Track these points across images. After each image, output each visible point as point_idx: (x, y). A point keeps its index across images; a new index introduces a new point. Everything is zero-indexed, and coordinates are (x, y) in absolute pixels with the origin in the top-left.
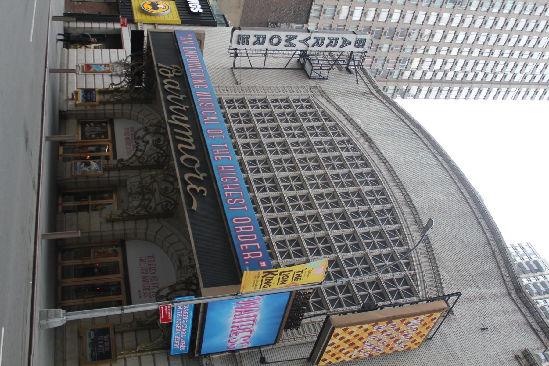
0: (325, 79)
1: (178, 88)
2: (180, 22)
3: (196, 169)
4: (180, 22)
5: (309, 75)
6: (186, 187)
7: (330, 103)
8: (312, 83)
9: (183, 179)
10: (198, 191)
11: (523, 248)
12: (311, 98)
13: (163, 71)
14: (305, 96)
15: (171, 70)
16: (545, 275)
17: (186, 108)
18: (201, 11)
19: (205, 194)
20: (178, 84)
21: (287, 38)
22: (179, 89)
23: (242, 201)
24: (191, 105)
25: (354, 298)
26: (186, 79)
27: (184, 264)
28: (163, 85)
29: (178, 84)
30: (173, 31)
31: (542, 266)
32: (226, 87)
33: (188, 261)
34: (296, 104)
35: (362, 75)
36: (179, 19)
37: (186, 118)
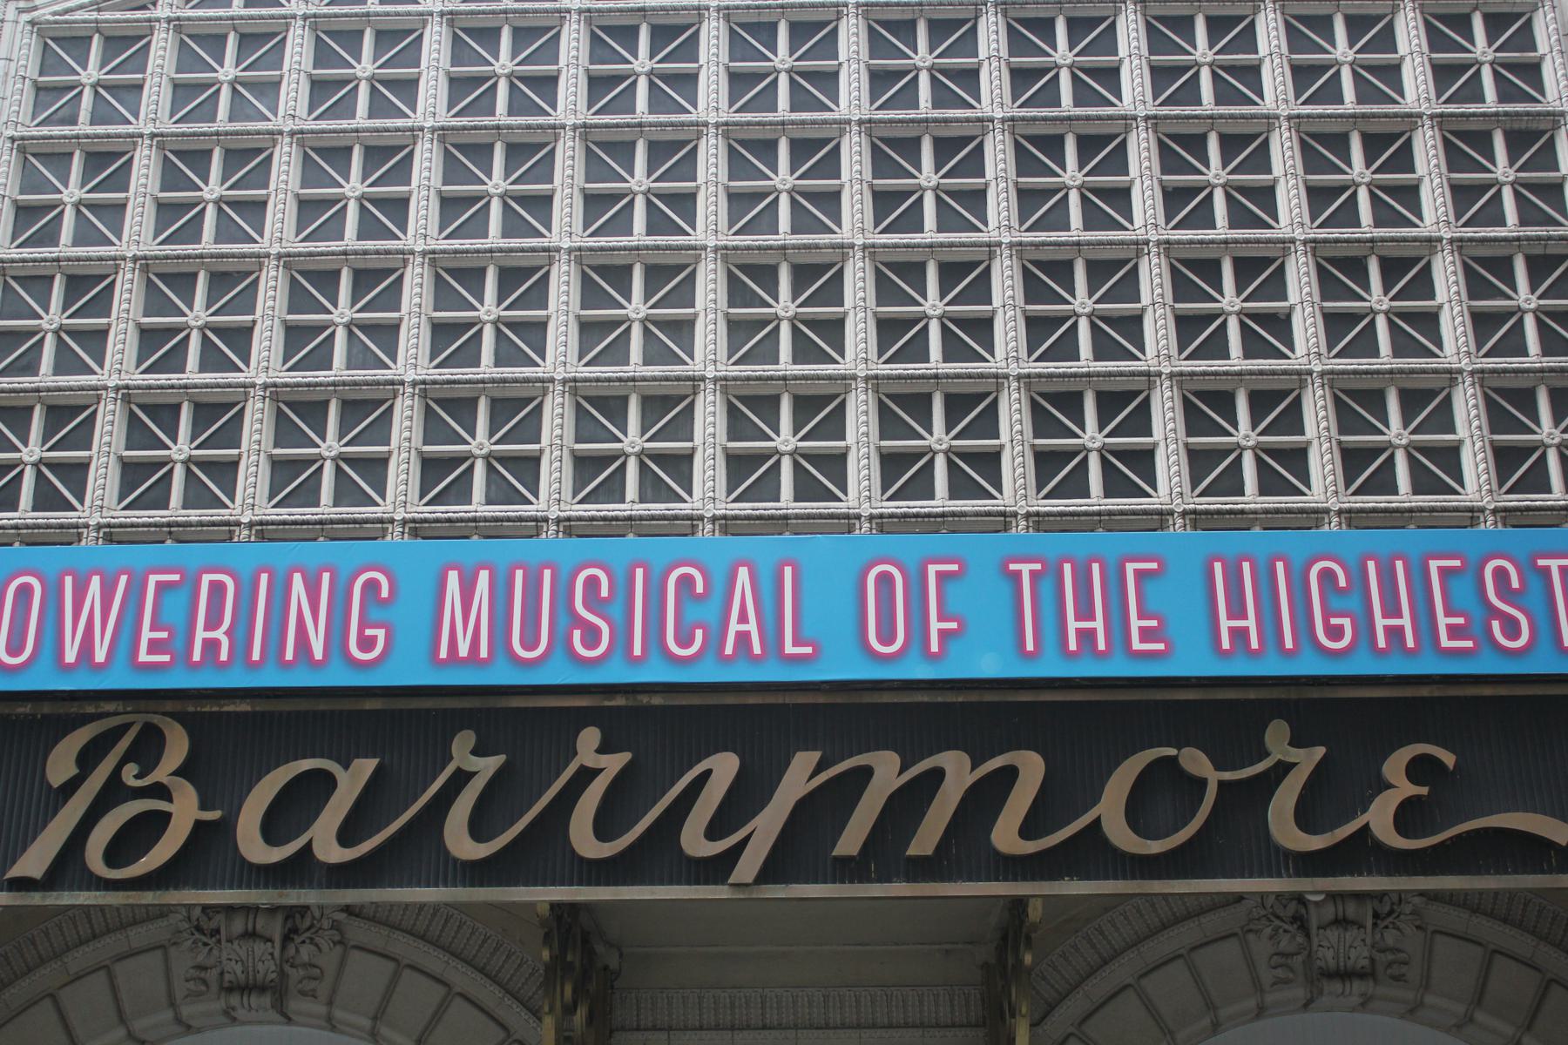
1: (353, 779)
3: (1228, 776)
6: (1380, 848)
9: (1309, 864)
10: (1413, 790)
13: (117, 853)
15: (114, 792)
17: (603, 749)
19: (1448, 759)
20: (306, 764)
22: (366, 767)
23: (1500, 574)
24: (583, 718)
25: (1538, 251)
26: (244, 707)
27: (1359, 956)
28: (301, 868)
29: (306, 764)
33: (1351, 934)
37: (724, 767)
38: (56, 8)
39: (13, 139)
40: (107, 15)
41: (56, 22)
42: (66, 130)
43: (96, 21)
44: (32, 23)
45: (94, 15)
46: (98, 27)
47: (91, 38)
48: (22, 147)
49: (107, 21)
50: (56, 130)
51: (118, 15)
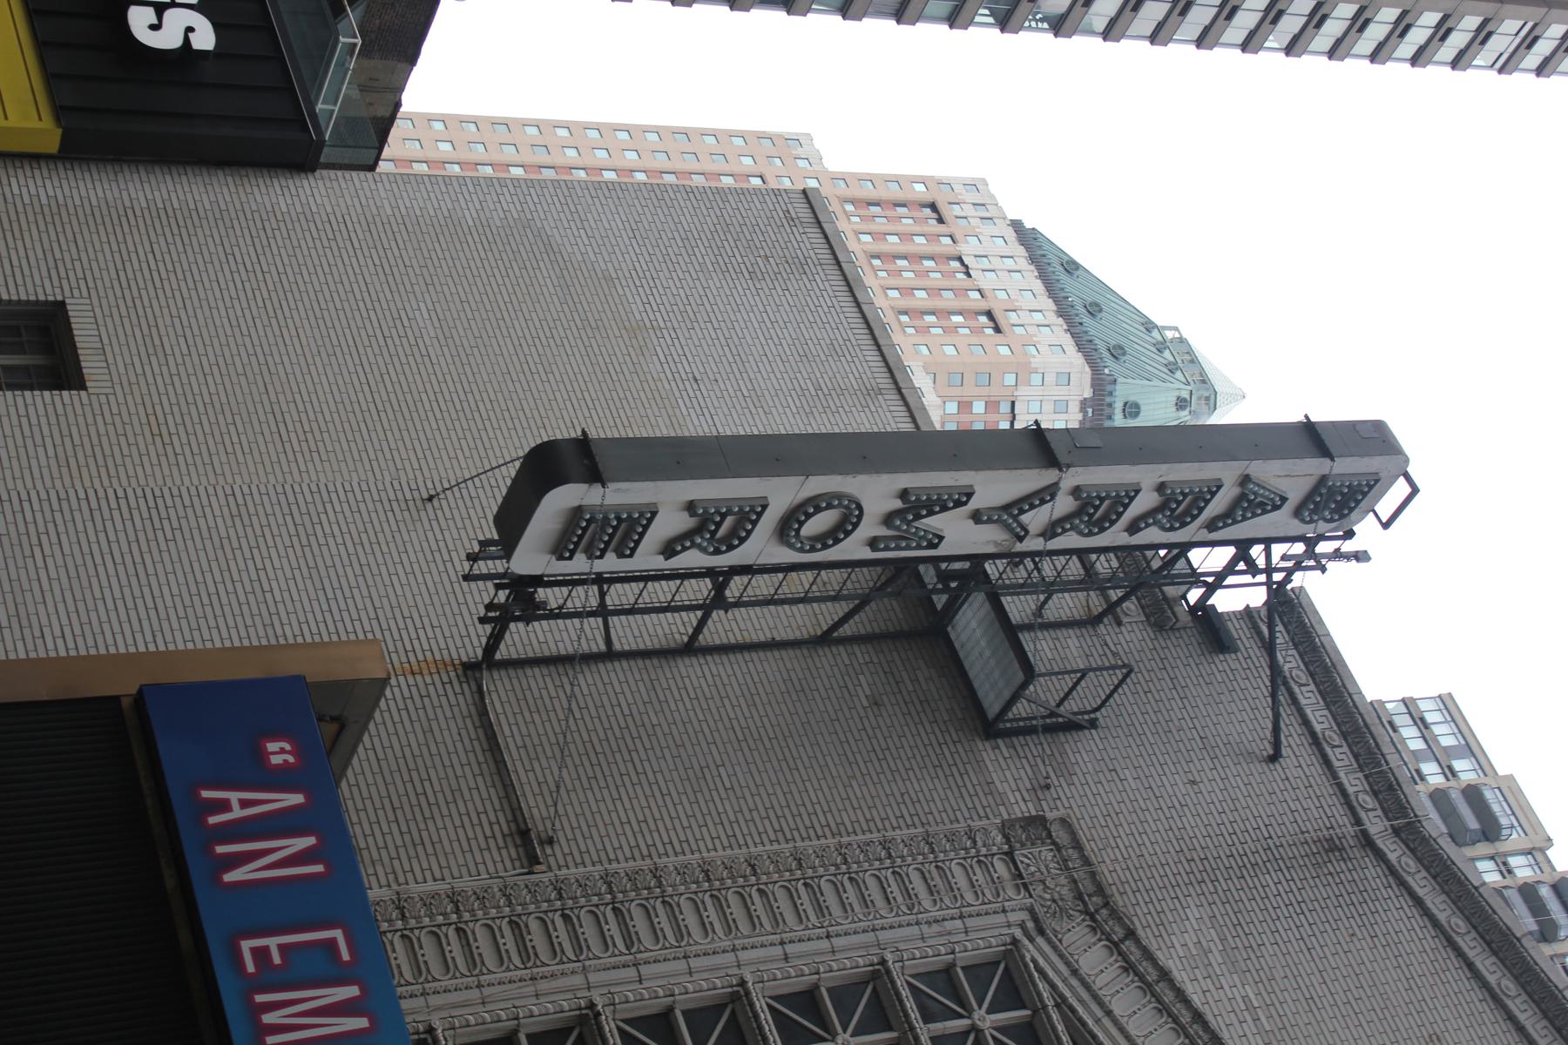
0: (1078, 727)
2: (44, 131)
4: (52, 144)
5: (992, 707)
7: (1147, 987)
8: (1008, 778)
11: (1421, 723)
12: (1030, 951)
14: (981, 936)
16: (1506, 855)
18: (205, 39)
21: (898, 504)
30: (125, 686)
31: (1496, 808)
32: (454, 898)
34: (939, 1027)
35: (1321, 720)
36: (47, 123)
38: (1041, 961)
39: (883, 962)
40: (1055, 1016)
41: (1026, 966)
42: (914, 1015)
43: (1045, 1007)
44: (1015, 942)
45: (1050, 1003)
46: (1039, 1010)
47: (1024, 1007)
48: (879, 976)
49: (1049, 1018)
50: (910, 1004)
51: (1060, 1028)
